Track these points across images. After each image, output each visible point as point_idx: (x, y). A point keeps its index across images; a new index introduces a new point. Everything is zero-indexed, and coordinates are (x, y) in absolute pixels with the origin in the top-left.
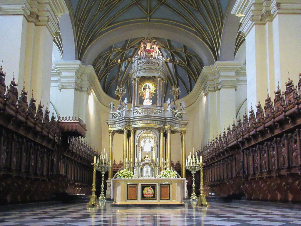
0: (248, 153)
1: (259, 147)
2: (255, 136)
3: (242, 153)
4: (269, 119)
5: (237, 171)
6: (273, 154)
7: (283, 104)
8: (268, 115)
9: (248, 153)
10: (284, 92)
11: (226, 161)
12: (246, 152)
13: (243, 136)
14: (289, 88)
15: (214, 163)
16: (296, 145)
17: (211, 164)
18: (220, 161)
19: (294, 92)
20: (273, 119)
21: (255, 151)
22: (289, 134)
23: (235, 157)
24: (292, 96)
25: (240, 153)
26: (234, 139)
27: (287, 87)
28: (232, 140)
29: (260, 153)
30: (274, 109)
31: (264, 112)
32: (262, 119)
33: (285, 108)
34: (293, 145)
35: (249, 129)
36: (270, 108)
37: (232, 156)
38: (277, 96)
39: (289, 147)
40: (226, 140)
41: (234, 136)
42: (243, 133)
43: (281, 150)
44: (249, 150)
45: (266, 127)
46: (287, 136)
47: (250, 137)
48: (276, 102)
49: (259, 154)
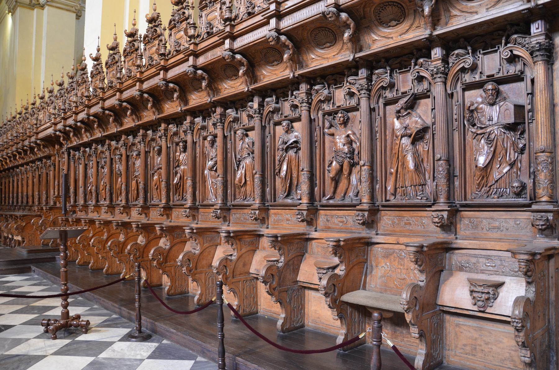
0: (77, 157)
1: (96, 149)
2: (88, 125)
3: (66, 156)
4: (111, 92)
5: (56, 194)
6: (119, 170)
7: (138, 62)
8: (112, 82)
9: (77, 157)
10: (142, 36)
11: (38, 168)
12: (74, 155)
13: (65, 119)
14: (152, 28)
15: (17, 167)
16: (160, 158)
17: (13, 168)
18: (27, 164)
19: (161, 41)
20: (118, 93)
21: (90, 155)
22: (148, 132)
23: (54, 161)
24: (154, 49)
25: (63, 153)
26: (48, 124)
27: (150, 25)
28: (46, 123)
29: (98, 163)
30: (124, 71)
31: (105, 73)
32: (100, 88)
33: (142, 73)
34: (156, 157)
35: (77, 107)
36: (115, 68)
37: (48, 157)
38: (130, 42)
39: (149, 160)
40: (35, 122)
41: (50, 117)
42: (65, 113)
43: (134, 164)
44: (79, 153)
45: (107, 109)
46: (145, 136)
47: (79, 124)
48: (127, 55)
49: (95, 165)
